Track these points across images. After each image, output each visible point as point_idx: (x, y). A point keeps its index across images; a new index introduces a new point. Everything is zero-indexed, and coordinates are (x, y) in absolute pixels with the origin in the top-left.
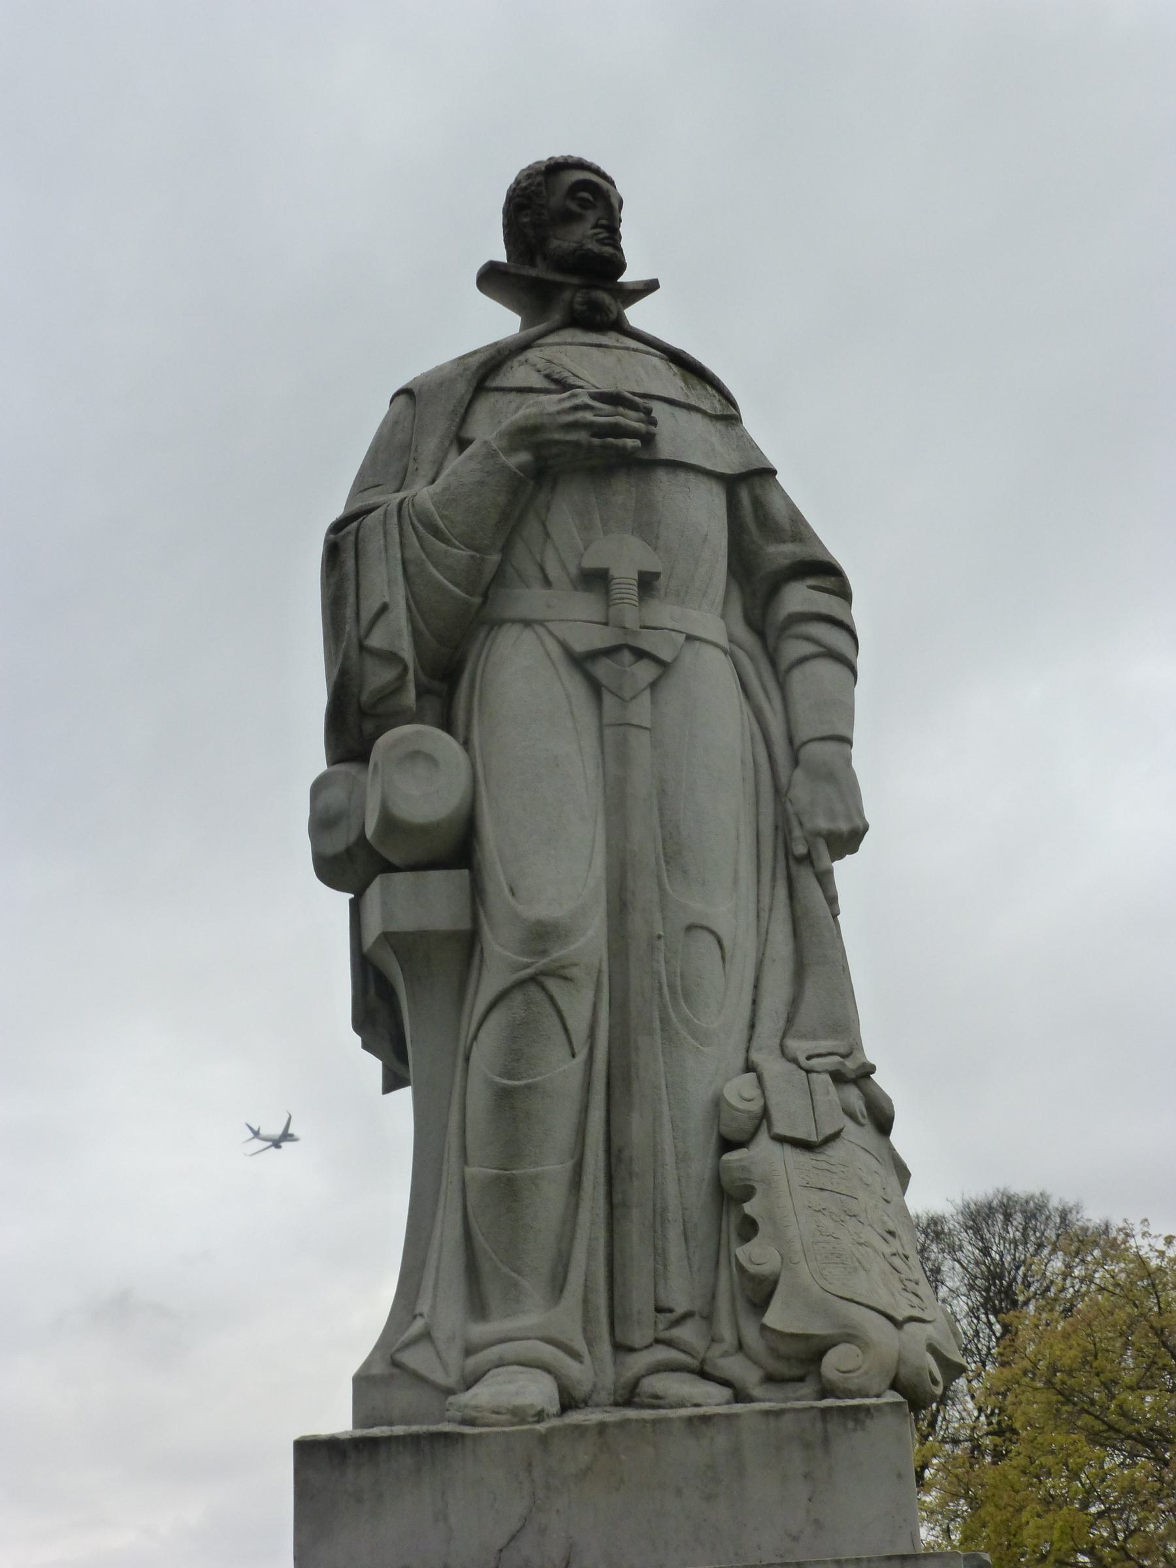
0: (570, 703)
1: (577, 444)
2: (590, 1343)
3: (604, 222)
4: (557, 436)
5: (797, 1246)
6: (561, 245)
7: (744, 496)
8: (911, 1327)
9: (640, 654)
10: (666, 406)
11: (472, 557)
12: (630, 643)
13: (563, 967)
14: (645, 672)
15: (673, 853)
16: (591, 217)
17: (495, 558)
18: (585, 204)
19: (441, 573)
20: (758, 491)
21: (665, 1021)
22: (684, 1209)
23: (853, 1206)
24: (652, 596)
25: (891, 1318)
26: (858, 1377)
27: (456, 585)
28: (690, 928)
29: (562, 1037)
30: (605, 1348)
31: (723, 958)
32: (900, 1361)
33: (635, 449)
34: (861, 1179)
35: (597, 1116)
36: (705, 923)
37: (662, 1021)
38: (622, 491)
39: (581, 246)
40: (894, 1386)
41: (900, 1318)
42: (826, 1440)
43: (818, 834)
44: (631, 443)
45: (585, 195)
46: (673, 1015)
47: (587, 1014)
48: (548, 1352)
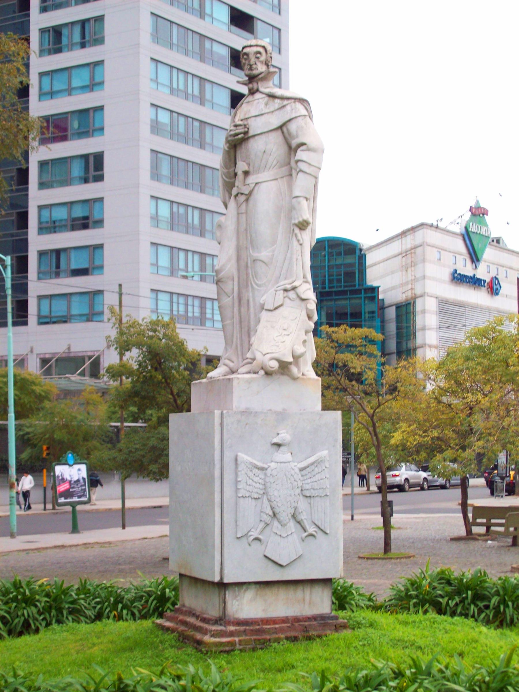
2: (238, 358)
28: (254, 261)
30: (240, 359)
32: (262, 362)
40: (262, 368)
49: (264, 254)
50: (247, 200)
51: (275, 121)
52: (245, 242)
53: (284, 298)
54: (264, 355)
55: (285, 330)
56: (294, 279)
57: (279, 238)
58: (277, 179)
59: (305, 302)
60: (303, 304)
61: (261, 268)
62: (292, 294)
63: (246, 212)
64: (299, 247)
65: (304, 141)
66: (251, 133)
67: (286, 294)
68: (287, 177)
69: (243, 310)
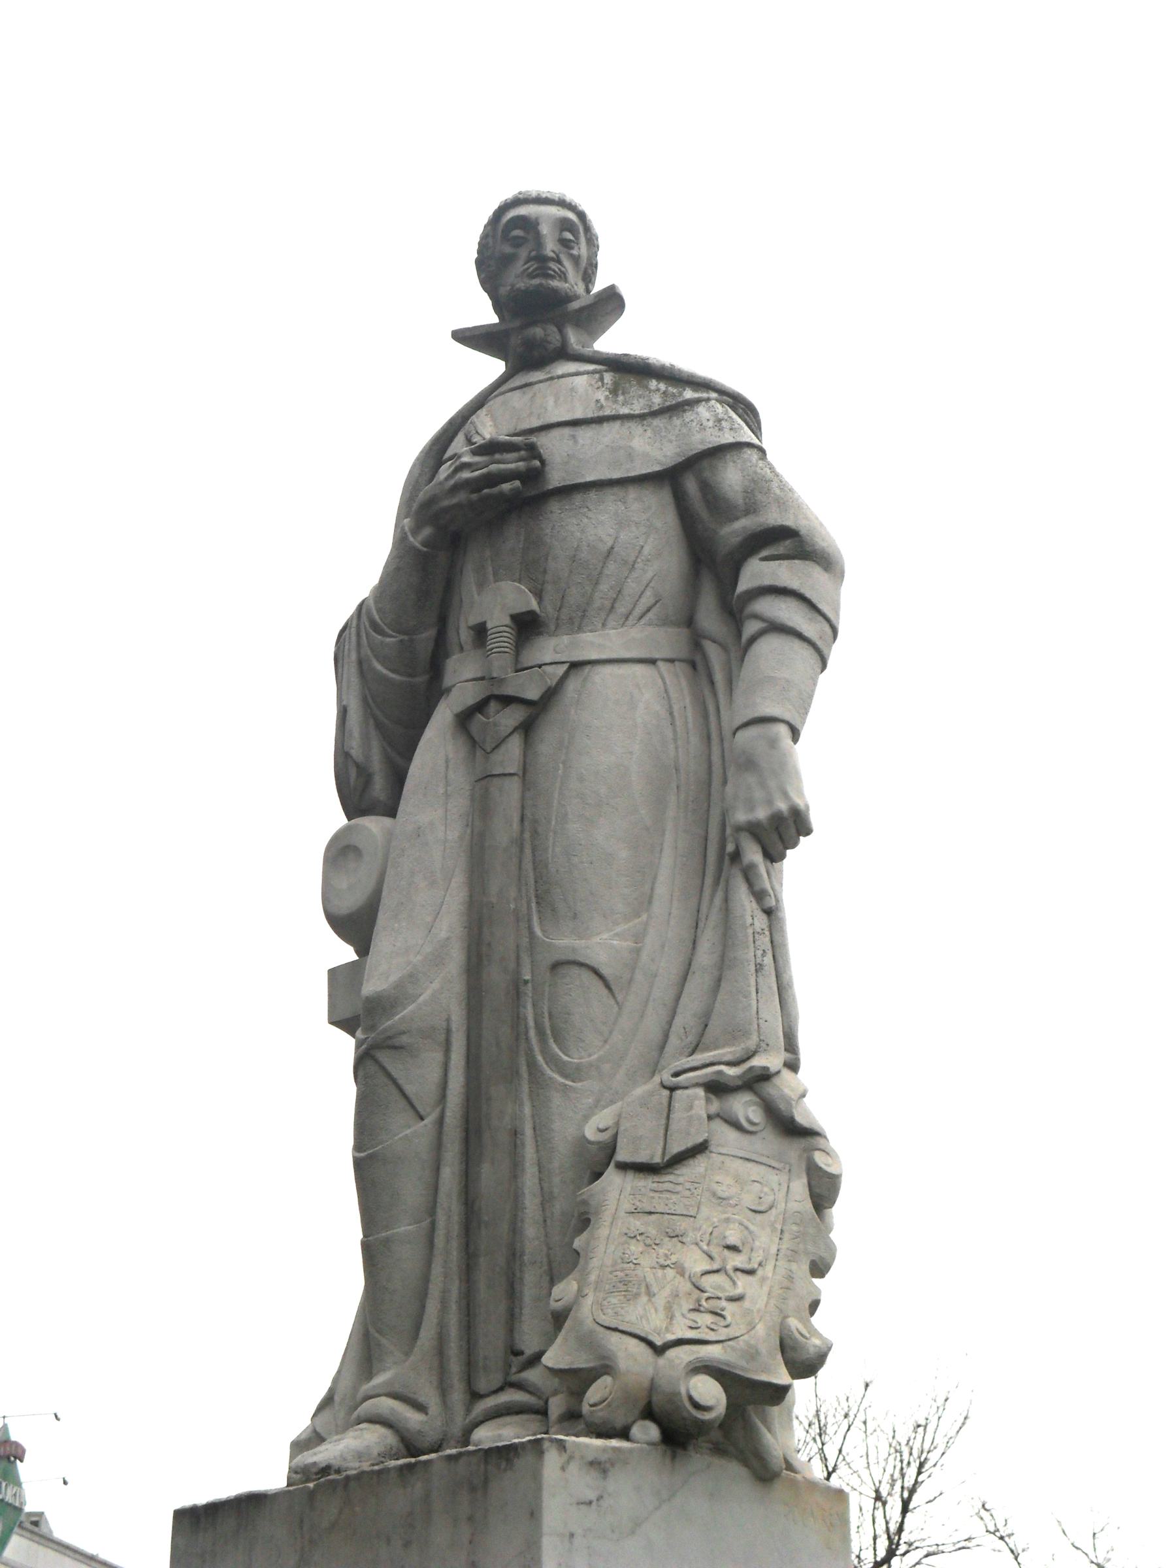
0: (447, 767)
1: (459, 506)
2: (443, 1391)
3: (533, 253)
4: (446, 503)
5: (593, 1277)
6: (536, 279)
7: (691, 485)
8: (672, 1353)
9: (507, 701)
10: (567, 431)
11: (401, 641)
12: (496, 692)
13: (390, 1038)
14: (510, 718)
15: (545, 894)
16: (523, 253)
17: (427, 635)
18: (518, 243)
19: (383, 665)
20: (707, 474)
21: (532, 1065)
22: (550, 1249)
23: (682, 1225)
24: (540, 634)
25: (650, 1344)
26: (602, 1410)
27: (393, 671)
28: (556, 966)
29: (402, 1103)
30: (458, 1396)
31: (608, 986)
32: (652, 1387)
33: (516, 493)
34: (714, 1194)
35: (450, 1174)
36: (571, 957)
37: (528, 1066)
38: (513, 538)
39: (513, 286)
40: (649, 1413)
41: (659, 1342)
42: (486, 1481)
43: (739, 829)
44: (506, 487)
45: (517, 232)
46: (540, 1058)
47: (435, 1075)
48: (386, 1405)
49: (603, 944)
50: (527, 729)
51: (653, 448)
52: (512, 893)
53: (710, 1118)
54: (659, 1350)
55: (733, 1248)
56: (752, 1043)
57: (662, 890)
58: (652, 662)
59: (803, 1143)
60: (793, 1149)
61: (582, 1000)
62: (744, 1107)
63: (525, 772)
64: (761, 921)
65: (789, 522)
66: (556, 478)
67: (715, 1106)
68: (683, 665)
69: (489, 1175)
